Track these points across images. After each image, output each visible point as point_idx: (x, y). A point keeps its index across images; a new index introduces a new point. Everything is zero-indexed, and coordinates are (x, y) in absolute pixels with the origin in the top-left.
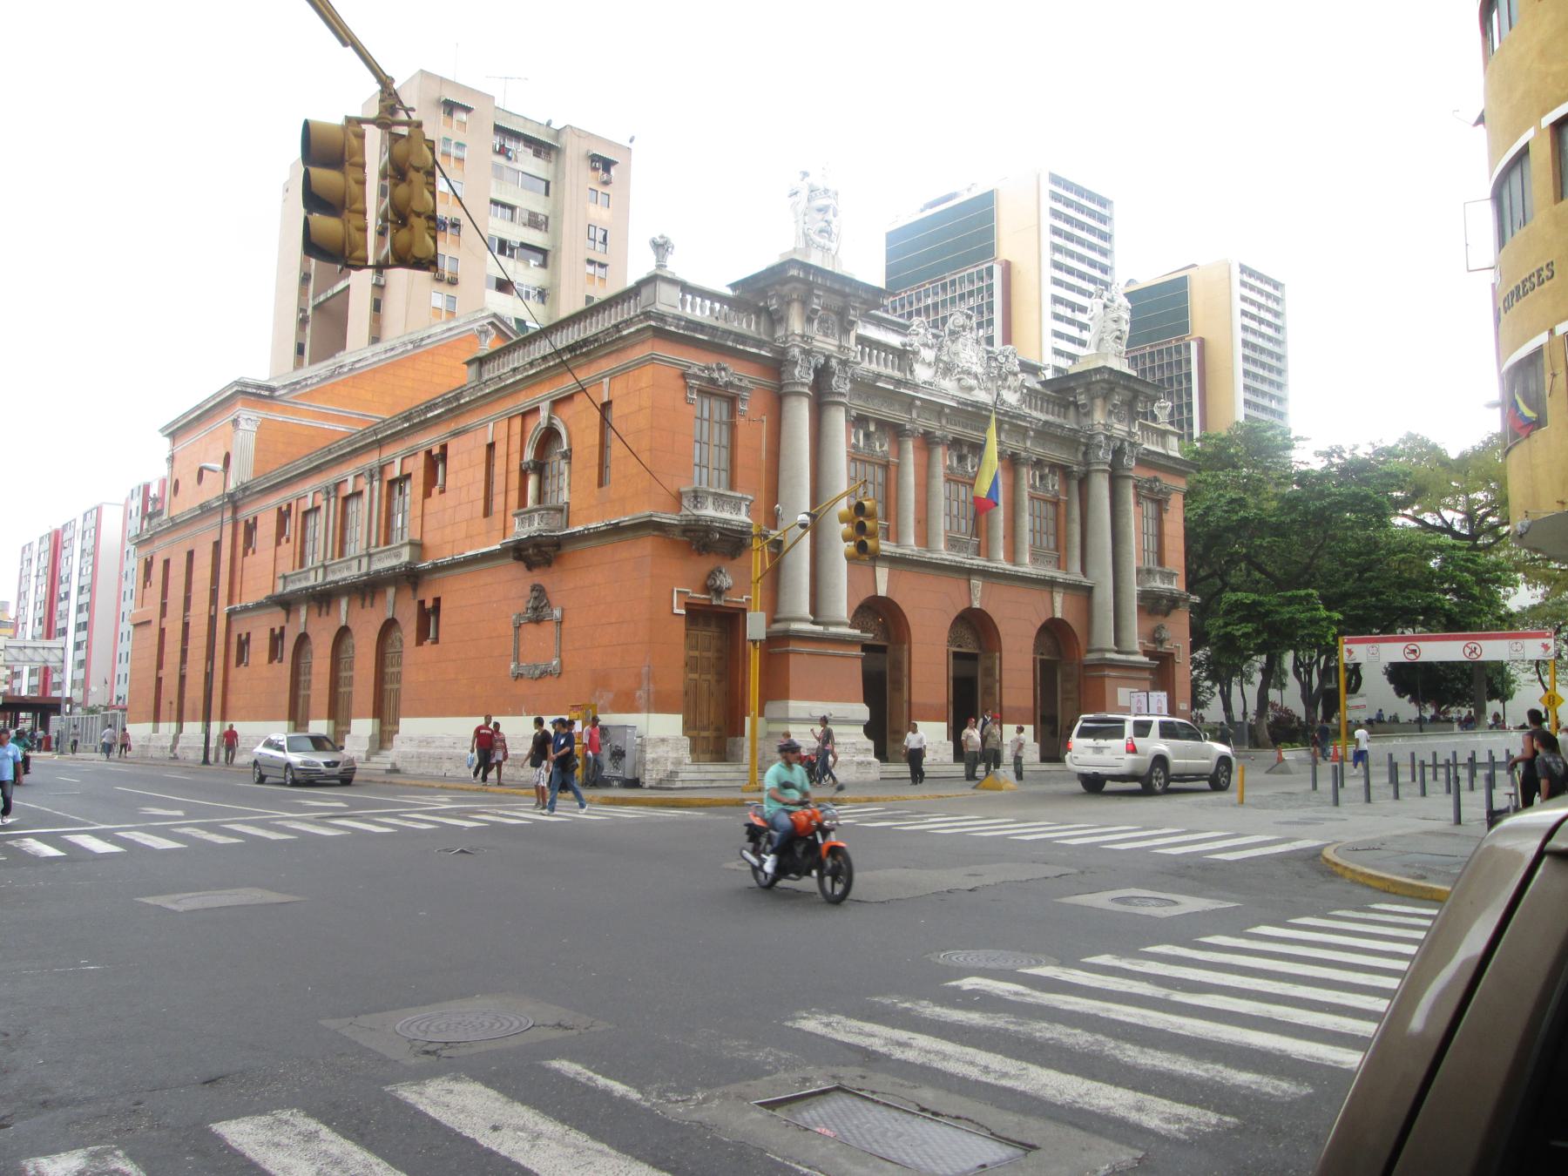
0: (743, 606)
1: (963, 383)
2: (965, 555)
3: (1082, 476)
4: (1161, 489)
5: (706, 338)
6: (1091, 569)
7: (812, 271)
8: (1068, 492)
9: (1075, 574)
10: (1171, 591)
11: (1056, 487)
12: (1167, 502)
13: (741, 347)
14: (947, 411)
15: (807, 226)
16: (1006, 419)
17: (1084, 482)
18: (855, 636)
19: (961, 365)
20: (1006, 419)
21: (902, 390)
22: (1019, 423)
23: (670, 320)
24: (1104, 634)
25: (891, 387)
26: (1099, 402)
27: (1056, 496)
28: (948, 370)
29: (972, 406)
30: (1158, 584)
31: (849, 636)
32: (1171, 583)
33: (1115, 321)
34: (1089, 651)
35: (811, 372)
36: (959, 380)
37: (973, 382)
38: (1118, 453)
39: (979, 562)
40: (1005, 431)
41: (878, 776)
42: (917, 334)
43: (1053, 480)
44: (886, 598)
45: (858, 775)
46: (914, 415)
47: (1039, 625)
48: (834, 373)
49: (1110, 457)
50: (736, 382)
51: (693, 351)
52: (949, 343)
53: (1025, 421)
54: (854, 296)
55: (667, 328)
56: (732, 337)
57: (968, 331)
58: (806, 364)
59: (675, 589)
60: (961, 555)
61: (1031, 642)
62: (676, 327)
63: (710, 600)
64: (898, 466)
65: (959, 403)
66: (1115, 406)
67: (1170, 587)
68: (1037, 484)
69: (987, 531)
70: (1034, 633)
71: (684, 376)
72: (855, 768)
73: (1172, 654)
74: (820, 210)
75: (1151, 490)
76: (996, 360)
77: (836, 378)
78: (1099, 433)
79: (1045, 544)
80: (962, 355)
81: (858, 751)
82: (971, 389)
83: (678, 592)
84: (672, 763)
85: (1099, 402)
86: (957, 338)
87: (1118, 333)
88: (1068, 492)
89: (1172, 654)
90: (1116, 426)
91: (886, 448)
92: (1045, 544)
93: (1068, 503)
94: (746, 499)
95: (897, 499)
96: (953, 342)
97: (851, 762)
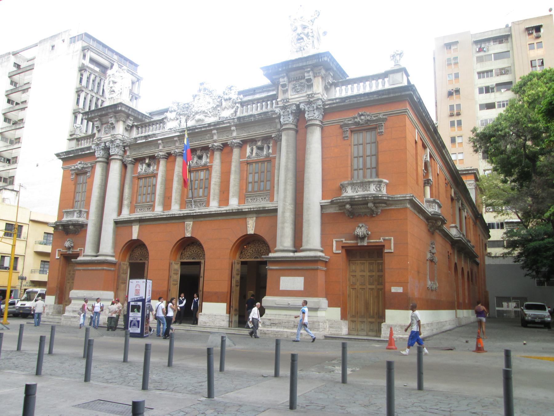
5: (72, 155)
7: (90, 113)
13: (84, 153)
20: (212, 128)
21: (149, 140)
22: (221, 126)
25: (144, 141)
50: (85, 166)
53: (224, 124)
56: (79, 151)
63: (67, 252)
67: (366, 193)
75: (357, 124)
90: (290, 97)
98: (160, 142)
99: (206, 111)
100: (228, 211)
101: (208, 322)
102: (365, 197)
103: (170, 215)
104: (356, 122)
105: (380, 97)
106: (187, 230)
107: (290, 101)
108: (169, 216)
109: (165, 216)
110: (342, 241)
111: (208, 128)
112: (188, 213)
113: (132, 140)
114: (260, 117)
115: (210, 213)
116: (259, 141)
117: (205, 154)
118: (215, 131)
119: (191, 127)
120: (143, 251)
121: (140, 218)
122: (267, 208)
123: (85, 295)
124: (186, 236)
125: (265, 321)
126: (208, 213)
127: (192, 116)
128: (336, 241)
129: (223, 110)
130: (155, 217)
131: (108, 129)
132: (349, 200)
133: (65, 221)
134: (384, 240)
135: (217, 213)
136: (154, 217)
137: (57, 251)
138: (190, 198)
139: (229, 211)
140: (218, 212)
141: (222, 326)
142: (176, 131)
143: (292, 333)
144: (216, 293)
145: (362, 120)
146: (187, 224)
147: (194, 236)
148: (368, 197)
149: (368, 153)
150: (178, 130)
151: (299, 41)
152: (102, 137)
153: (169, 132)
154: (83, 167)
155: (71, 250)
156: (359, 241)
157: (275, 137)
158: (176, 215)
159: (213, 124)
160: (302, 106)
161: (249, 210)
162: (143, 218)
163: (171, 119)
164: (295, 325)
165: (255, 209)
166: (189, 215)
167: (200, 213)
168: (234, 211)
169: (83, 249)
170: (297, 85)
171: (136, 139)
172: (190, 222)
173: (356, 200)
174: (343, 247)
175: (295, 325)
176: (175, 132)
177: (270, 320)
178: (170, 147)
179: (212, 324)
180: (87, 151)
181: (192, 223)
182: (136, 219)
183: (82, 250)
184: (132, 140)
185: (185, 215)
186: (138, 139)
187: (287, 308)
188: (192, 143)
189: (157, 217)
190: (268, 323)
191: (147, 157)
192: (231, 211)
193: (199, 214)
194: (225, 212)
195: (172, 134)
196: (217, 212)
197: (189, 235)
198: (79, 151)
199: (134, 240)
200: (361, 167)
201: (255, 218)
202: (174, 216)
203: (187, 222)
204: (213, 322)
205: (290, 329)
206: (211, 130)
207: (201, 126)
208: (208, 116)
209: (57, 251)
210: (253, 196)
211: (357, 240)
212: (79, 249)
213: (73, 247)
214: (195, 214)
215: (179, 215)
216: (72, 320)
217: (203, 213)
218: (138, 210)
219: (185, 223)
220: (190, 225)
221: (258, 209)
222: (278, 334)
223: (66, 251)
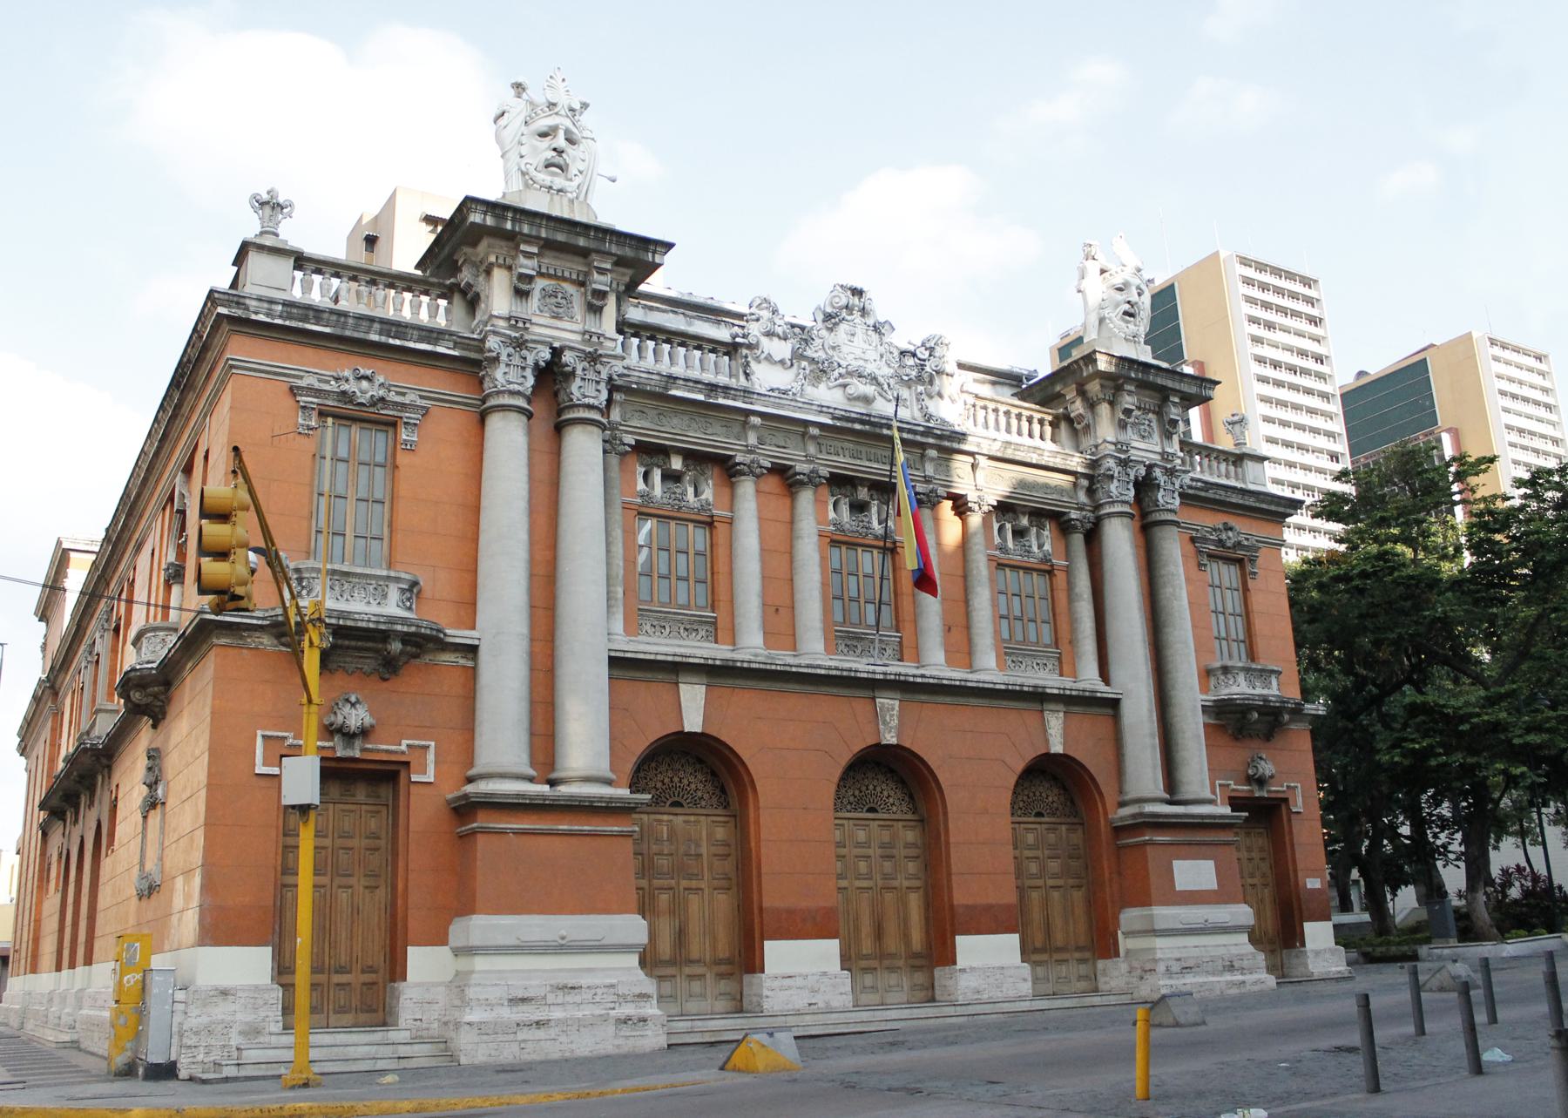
0: (403, 759)
1: (850, 390)
2: (871, 660)
3: (1089, 526)
4: (1239, 543)
5: (327, 330)
6: (1116, 672)
7: (510, 215)
8: (1068, 555)
9: (1088, 678)
10: (1265, 699)
11: (1047, 547)
12: (1252, 561)
13: (398, 342)
14: (814, 431)
15: (525, 160)
16: (931, 441)
17: (1093, 536)
18: (620, 799)
19: (844, 363)
20: (931, 441)
21: (721, 401)
23: (254, 303)
24: (1145, 776)
25: (701, 397)
26: (1104, 409)
27: (1046, 559)
28: (821, 371)
29: (862, 422)
30: (1239, 688)
31: (601, 799)
32: (1268, 686)
33: (1120, 289)
34: (1122, 804)
35: (529, 373)
36: (845, 386)
37: (869, 390)
38: (1145, 486)
39: (896, 669)
40: (932, 459)
41: (662, 1041)
42: (758, 320)
43: (1038, 536)
44: (702, 734)
45: (617, 1042)
46: (752, 439)
47: (1020, 766)
48: (573, 374)
49: (1132, 493)
50: (393, 397)
51: (309, 353)
52: (824, 333)
54: (598, 252)
55: (253, 317)
56: (377, 326)
57: (857, 314)
58: (516, 360)
59: (259, 733)
60: (865, 660)
61: (1007, 796)
62: (267, 315)
64: (730, 522)
65: (834, 418)
66: (1128, 412)
67: (1265, 692)
68: (1010, 544)
69: (915, 622)
70: (1013, 780)
71: (293, 391)
72: (611, 1029)
73: (1286, 800)
74: (543, 135)
75: (1221, 543)
76: (914, 355)
77: (578, 382)
78: (1105, 456)
79: (1033, 638)
80: (845, 349)
81: (623, 999)
82: (867, 400)
83: (263, 736)
84: (240, 1033)
85: (1104, 409)
86: (835, 324)
87: (1127, 307)
88: (1068, 555)
89: (1286, 800)
90: (1135, 444)
91: (708, 494)
92: (1033, 638)
93: (1068, 571)
94: (398, 580)
95: (731, 573)
96: (830, 330)
97: (604, 1019)
98: (756, 420)
99: (881, 380)
100: (1010, 687)
101: (985, 990)
102: (1284, 702)
103: (842, 670)
104: (1220, 541)
105: (1257, 505)
106: (885, 723)
107: (1132, 451)
108: (838, 673)
109: (823, 672)
110: (1229, 785)
111: (919, 438)
112: (900, 675)
113: (654, 377)
114: (1052, 459)
115: (963, 683)
116: (1024, 514)
117: (876, 502)
118: (933, 453)
119: (874, 416)
120: (681, 774)
121: (725, 663)
122: (1099, 695)
123: (564, 933)
124: (884, 742)
125: (1170, 963)
126: (958, 683)
127: (836, 374)
128: (1220, 785)
129: (931, 397)
130: (788, 669)
131: (564, 302)
132: (1261, 703)
133: (373, 619)
134: (1288, 787)
135: (983, 688)
136: (782, 668)
137: (259, 741)
138: (869, 627)
139: (1014, 687)
140: (986, 686)
141: (1023, 994)
142: (824, 409)
143: (1228, 983)
144: (988, 908)
145: (1229, 538)
146: (883, 704)
147: (907, 744)
148: (1288, 703)
149: (1230, 609)
150: (831, 411)
151: (1127, 318)
152: (535, 320)
153: (800, 405)
154: (382, 399)
155: (358, 743)
156: (1255, 787)
157: (1077, 520)
158: (859, 675)
159: (939, 432)
160: (1158, 473)
161: (1062, 692)
162: (739, 664)
163: (769, 358)
164: (1224, 967)
165: (1074, 693)
166: (899, 681)
167: (936, 681)
168: (1026, 689)
169: (433, 744)
170: (1147, 422)
171: (672, 379)
172: (891, 702)
173: (1272, 704)
174: (1230, 798)
175: (1224, 967)
176: (821, 412)
177: (1179, 960)
178: (784, 447)
179: (998, 995)
180: (420, 340)
181: (897, 703)
182: (710, 662)
183: (428, 747)
184: (654, 377)
185: (888, 677)
186: (681, 382)
187: (1201, 929)
188: (858, 462)
189: (794, 669)
190: (1176, 967)
191: (679, 451)
192: (1018, 688)
193: (931, 681)
194: (1003, 687)
195: (808, 413)
196: (981, 685)
197: (894, 741)
198: (377, 326)
199: (690, 734)
200: (1223, 634)
201: (1061, 715)
202: (853, 674)
203: (882, 700)
204: (998, 987)
205: (1218, 975)
206: (923, 446)
207: (905, 426)
208: (885, 398)
209: (259, 741)
210: (1017, 655)
211: (1250, 785)
212: (405, 742)
213: (364, 733)
214: (919, 680)
215: (870, 676)
216: (521, 1036)
217: (945, 682)
218: (648, 627)
219: (878, 700)
220: (893, 709)
221: (1081, 693)
222: (1204, 988)
223: (331, 744)
